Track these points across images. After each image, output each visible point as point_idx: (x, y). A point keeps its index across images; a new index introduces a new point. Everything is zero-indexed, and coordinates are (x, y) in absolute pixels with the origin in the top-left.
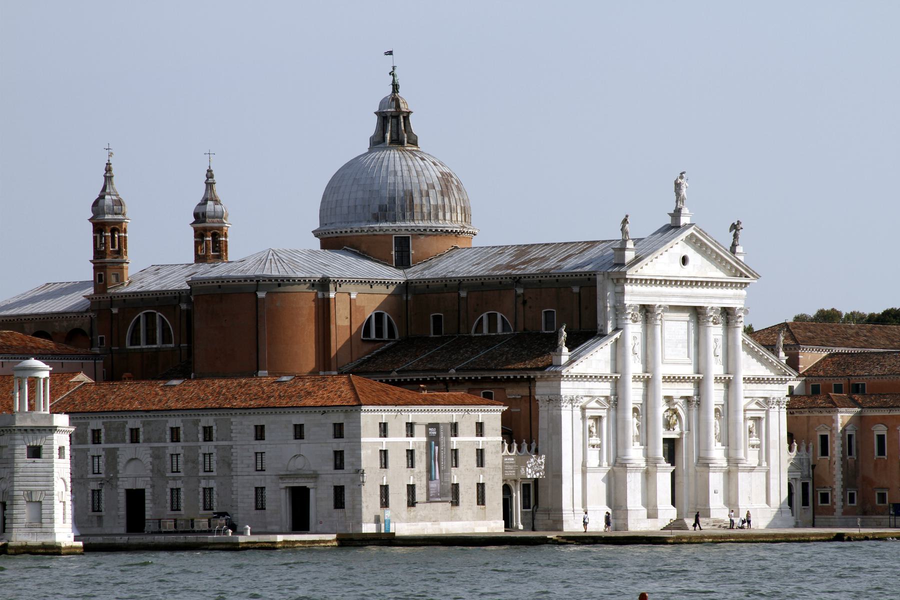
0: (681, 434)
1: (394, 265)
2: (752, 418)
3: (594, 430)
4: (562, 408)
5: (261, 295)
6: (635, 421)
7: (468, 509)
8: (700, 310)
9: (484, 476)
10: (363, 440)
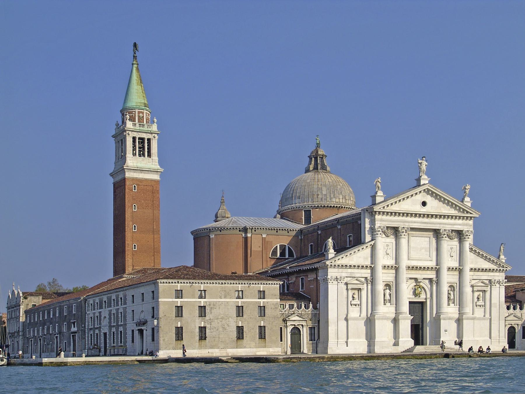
0: (426, 299)
1: (304, 224)
2: (478, 291)
3: (356, 296)
4: (329, 283)
5: (212, 236)
6: (388, 291)
7: (251, 341)
8: (438, 231)
9: (264, 322)
10: (160, 300)
